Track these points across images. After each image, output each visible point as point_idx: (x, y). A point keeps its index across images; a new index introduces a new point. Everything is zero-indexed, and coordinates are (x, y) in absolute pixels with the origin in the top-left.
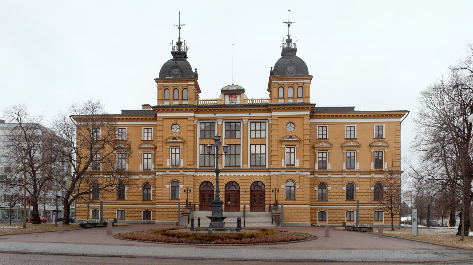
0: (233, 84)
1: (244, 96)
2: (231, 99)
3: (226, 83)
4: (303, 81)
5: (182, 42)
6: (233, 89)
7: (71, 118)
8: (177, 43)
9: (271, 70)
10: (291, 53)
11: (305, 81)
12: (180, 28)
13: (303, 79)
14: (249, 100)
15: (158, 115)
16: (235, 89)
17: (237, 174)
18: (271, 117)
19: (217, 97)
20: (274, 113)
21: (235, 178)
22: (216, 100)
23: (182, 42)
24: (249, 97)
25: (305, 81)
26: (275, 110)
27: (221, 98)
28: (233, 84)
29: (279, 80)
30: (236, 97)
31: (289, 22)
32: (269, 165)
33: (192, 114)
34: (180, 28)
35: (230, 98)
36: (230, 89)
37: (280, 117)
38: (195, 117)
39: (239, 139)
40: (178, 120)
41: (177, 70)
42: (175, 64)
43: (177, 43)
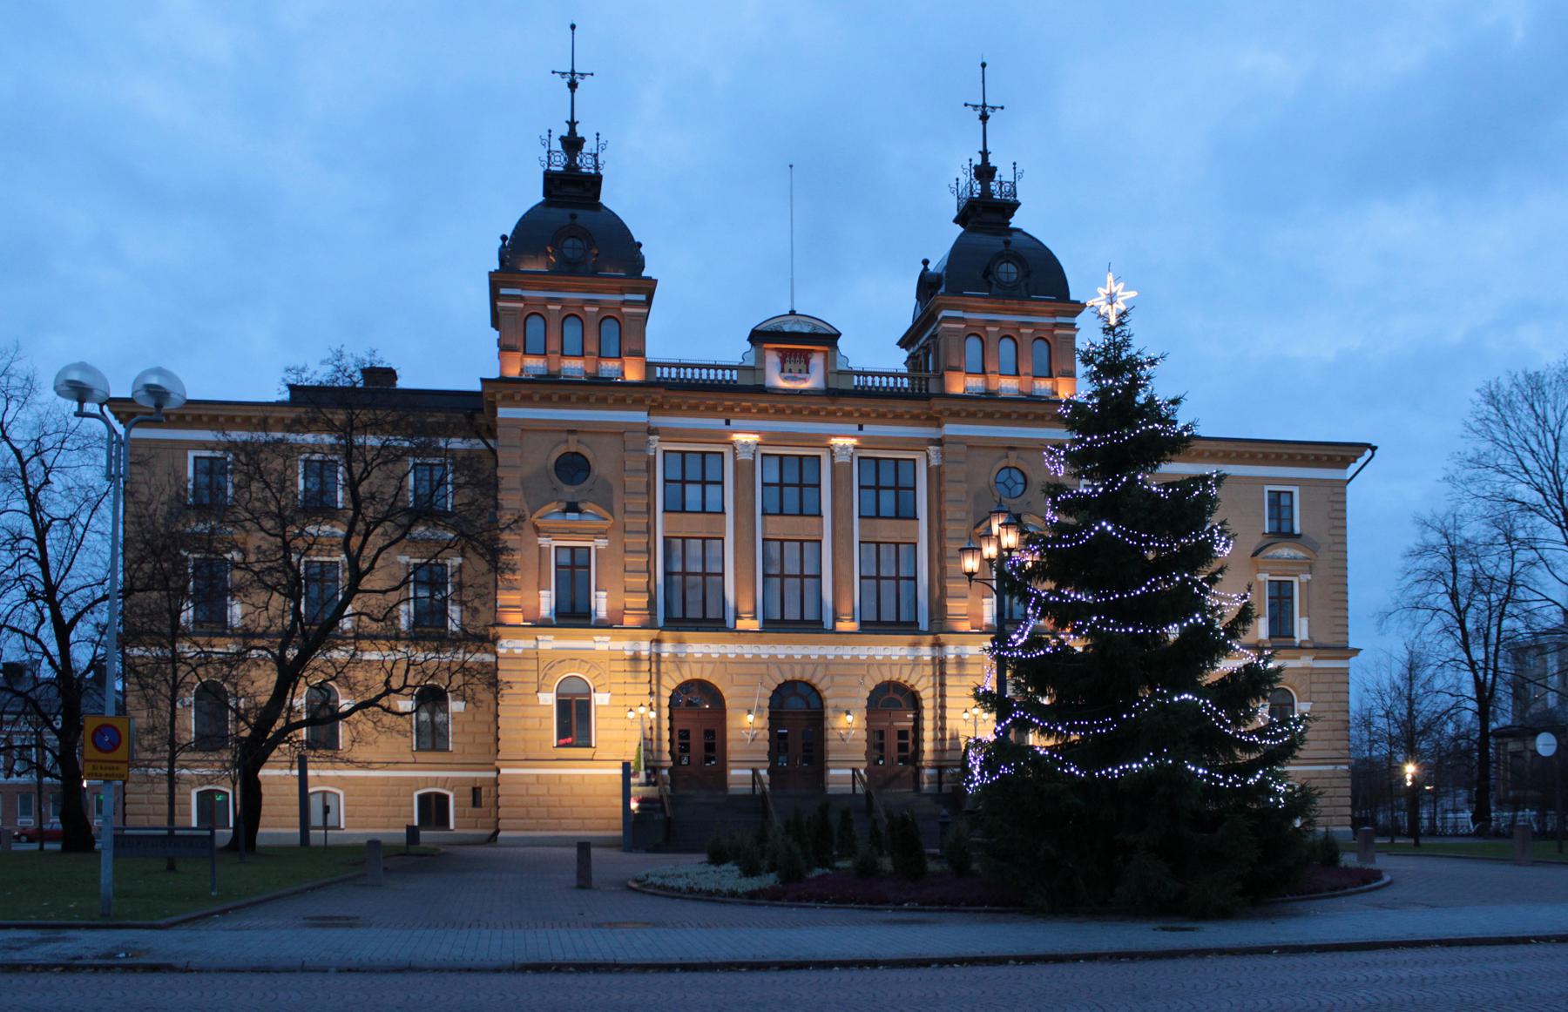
0: (792, 313)
1: (839, 359)
2: (788, 366)
3: (770, 308)
4: (1052, 321)
5: (582, 140)
6: (797, 328)
7: (105, 408)
8: (562, 139)
9: (926, 269)
10: (995, 217)
11: (1060, 320)
12: (573, 86)
13: (1054, 314)
14: (859, 374)
15: (503, 412)
16: (806, 330)
17: (814, 651)
18: (939, 442)
19: (735, 359)
20: (951, 429)
21: (809, 669)
22: (731, 368)
23: (582, 140)
24: (855, 364)
25: (1060, 320)
26: (956, 416)
27: (751, 363)
28: (792, 313)
29: (965, 309)
30: (807, 362)
31: (984, 106)
32: (931, 621)
33: (640, 416)
34: (573, 86)
35: (783, 361)
36: (787, 328)
37: (972, 445)
38: (652, 431)
39: (816, 520)
40: (586, 438)
41: (572, 240)
42: (569, 220)
43: (562, 139)
